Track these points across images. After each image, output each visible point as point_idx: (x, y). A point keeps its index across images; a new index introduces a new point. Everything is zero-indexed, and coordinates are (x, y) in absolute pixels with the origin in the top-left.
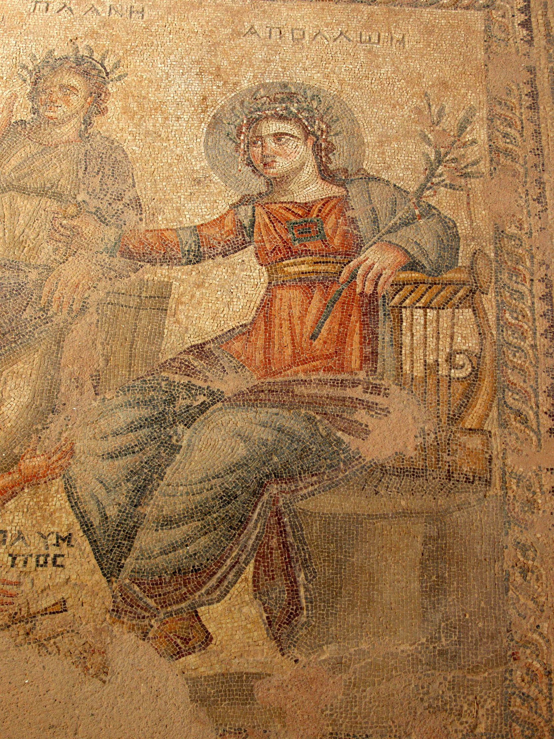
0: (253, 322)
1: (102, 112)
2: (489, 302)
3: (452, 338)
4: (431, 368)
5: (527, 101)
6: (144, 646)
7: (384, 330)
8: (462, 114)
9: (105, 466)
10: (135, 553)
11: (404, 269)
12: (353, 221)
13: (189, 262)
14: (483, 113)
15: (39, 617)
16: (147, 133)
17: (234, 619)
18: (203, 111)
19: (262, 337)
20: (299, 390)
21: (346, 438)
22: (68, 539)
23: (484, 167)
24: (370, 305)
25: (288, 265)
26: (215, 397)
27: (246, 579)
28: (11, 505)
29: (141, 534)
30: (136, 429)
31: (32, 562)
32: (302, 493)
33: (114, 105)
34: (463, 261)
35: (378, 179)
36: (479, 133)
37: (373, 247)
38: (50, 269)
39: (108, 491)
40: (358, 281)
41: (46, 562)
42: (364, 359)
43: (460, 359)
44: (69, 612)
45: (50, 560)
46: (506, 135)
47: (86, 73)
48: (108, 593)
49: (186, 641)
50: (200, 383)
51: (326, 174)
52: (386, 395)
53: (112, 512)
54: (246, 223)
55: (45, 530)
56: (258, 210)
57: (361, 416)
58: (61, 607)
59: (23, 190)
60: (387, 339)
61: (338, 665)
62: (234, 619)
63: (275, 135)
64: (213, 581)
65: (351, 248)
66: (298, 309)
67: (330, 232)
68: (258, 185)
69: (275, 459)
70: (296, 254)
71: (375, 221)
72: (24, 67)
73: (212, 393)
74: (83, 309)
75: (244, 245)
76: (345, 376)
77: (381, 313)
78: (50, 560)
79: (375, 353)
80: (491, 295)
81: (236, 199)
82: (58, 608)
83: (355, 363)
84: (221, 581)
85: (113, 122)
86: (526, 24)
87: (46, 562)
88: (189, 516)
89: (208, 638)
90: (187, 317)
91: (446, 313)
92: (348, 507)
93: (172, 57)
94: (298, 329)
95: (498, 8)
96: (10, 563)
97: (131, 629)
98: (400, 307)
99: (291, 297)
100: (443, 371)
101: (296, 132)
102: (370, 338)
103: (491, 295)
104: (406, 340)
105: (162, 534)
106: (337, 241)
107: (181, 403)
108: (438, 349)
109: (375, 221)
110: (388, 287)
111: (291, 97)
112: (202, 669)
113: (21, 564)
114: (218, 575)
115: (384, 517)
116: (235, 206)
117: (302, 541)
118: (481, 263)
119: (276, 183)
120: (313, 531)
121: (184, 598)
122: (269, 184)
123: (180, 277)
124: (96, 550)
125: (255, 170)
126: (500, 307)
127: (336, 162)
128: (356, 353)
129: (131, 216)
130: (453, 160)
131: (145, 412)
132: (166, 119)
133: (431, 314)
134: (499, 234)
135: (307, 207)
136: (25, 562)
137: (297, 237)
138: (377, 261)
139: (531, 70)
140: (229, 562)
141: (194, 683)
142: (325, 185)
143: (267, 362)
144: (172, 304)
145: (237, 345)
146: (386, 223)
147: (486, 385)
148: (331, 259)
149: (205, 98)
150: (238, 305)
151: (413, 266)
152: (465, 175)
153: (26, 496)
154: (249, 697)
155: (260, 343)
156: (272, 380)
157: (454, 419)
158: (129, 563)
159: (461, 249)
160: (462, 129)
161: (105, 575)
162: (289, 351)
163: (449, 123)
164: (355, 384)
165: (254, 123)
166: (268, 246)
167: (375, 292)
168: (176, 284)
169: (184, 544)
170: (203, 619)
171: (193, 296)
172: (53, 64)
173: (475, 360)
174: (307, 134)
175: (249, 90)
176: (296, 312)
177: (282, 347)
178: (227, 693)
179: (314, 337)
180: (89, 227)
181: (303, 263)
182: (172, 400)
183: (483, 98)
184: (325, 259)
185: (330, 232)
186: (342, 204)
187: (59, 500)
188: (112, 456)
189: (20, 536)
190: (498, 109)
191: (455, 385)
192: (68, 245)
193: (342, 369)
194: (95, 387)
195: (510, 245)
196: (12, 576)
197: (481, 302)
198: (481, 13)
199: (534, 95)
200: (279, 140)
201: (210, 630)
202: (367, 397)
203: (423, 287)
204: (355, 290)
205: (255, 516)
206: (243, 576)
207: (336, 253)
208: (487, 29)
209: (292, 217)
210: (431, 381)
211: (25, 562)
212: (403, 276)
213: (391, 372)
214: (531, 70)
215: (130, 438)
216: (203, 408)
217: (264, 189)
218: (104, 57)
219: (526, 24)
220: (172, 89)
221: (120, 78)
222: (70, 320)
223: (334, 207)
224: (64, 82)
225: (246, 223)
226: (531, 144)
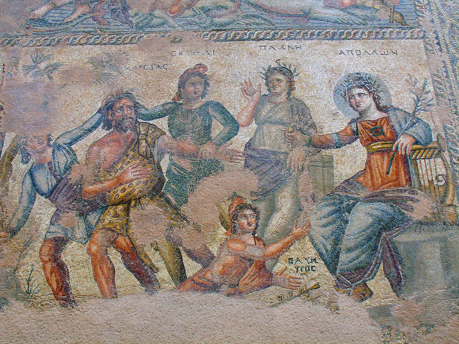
0: (365, 170)
1: (294, 89)
2: (446, 155)
3: (436, 170)
4: (431, 182)
5: (445, 74)
6: (351, 299)
7: (412, 169)
8: (423, 81)
9: (322, 230)
10: (340, 263)
11: (414, 144)
12: (393, 126)
13: (337, 147)
14: (430, 80)
15: (310, 291)
16: (312, 97)
17: (379, 284)
18: (331, 86)
19: (369, 175)
20: (387, 195)
21: (405, 212)
22: (315, 260)
23: (434, 102)
24: (405, 159)
25: (373, 146)
26: (357, 200)
27: (381, 270)
28: (292, 248)
29: (341, 255)
30: (331, 215)
31: (304, 270)
32: (394, 234)
33: (297, 86)
34: (434, 139)
35: (398, 109)
36: (430, 88)
37: (402, 136)
38: (287, 154)
39: (326, 239)
40: (399, 150)
41: (309, 269)
42: (407, 181)
43: (440, 178)
44: (321, 288)
45: (310, 268)
46: (440, 89)
47: (284, 74)
48: (334, 279)
49: (364, 295)
50: (350, 195)
51: (379, 108)
52: (417, 194)
53: (329, 247)
54: (355, 129)
55: (307, 256)
56: (358, 125)
57: (409, 202)
58: (317, 286)
59: (270, 122)
60: (414, 172)
61: (418, 300)
62: (379, 284)
63: (358, 94)
64: (369, 272)
65: (394, 137)
66: (381, 163)
67: (385, 131)
68: (356, 115)
69: (382, 223)
70: (375, 141)
71: (400, 126)
72: (261, 73)
73: (355, 199)
74: (303, 169)
75: (356, 139)
76: (401, 188)
77: (409, 162)
78: (310, 268)
79: (410, 178)
80: (446, 152)
81: (349, 121)
82: (317, 286)
83: (404, 183)
84: (372, 271)
85: (298, 93)
86: (438, 44)
87: (309, 269)
88: (356, 247)
89: (372, 293)
90: (341, 169)
91: (432, 160)
92: (411, 239)
93: (315, 65)
94: (381, 170)
95: (427, 38)
96: (296, 271)
97: (344, 293)
98: (415, 159)
99: (376, 157)
100: (435, 183)
101: (366, 92)
102: (408, 173)
103: (446, 152)
104: (420, 172)
105: (348, 255)
106: (388, 135)
107: (345, 204)
108: (432, 175)
109: (400, 126)
110: (410, 152)
111: (361, 78)
112: (372, 305)
113: (300, 271)
114: (371, 269)
115: (425, 241)
116: (350, 124)
117: (397, 253)
118: (440, 141)
119: (361, 114)
120: (401, 249)
121: (361, 279)
122: (360, 114)
123: (334, 152)
124: (326, 263)
125: (354, 109)
126: (451, 156)
127: (383, 103)
128: (404, 178)
129: (312, 131)
130: (423, 100)
131: (333, 208)
132: (318, 90)
133: (427, 161)
134: (445, 127)
135: (375, 122)
136: (302, 270)
137: (374, 134)
138: (404, 141)
139: (444, 62)
140: (374, 263)
141: (369, 310)
142: (380, 113)
143: (373, 184)
144: (335, 165)
145: (361, 179)
146: (404, 126)
147: (451, 187)
148: (388, 142)
149: (330, 81)
150: (359, 163)
151: (417, 143)
152: (429, 105)
153: (297, 244)
154: (389, 315)
155: (369, 177)
156: (376, 191)
157: (442, 202)
158: (339, 267)
159: (433, 135)
160: (424, 88)
161: (331, 273)
162: (380, 180)
163: (419, 85)
164: (405, 191)
165: (349, 89)
166: (364, 139)
167: (406, 154)
168: (334, 156)
169: (357, 257)
170: (368, 286)
171: (341, 160)
172: (271, 71)
173: (445, 177)
174: (370, 93)
175: (345, 77)
176: (379, 163)
177: (377, 179)
178: (381, 313)
179: (388, 173)
180: (299, 136)
181: (378, 144)
182: (342, 203)
183: (429, 74)
184: (385, 142)
185: (385, 131)
186: (387, 120)
187: (309, 245)
188: (325, 226)
189: (298, 260)
190: (436, 78)
191: (441, 189)
192: (292, 144)
193: (400, 185)
194: (313, 199)
195: (449, 132)
196: (298, 276)
197: (443, 155)
198: (421, 40)
199: (446, 72)
200: (360, 96)
201: (372, 290)
202: (409, 195)
203: (422, 151)
204: (398, 154)
205: (379, 246)
206: (380, 269)
207: (389, 140)
208: (425, 46)
209: (370, 126)
210: (432, 188)
211: (302, 270)
212: (415, 147)
213: (417, 186)
214: (444, 62)
215: (330, 219)
216: (354, 205)
217: (358, 116)
218: (290, 68)
219: (438, 44)
220: (317, 78)
221: (296, 75)
222: (299, 173)
223: (385, 121)
224: (278, 77)
225: (355, 130)
226: (449, 91)
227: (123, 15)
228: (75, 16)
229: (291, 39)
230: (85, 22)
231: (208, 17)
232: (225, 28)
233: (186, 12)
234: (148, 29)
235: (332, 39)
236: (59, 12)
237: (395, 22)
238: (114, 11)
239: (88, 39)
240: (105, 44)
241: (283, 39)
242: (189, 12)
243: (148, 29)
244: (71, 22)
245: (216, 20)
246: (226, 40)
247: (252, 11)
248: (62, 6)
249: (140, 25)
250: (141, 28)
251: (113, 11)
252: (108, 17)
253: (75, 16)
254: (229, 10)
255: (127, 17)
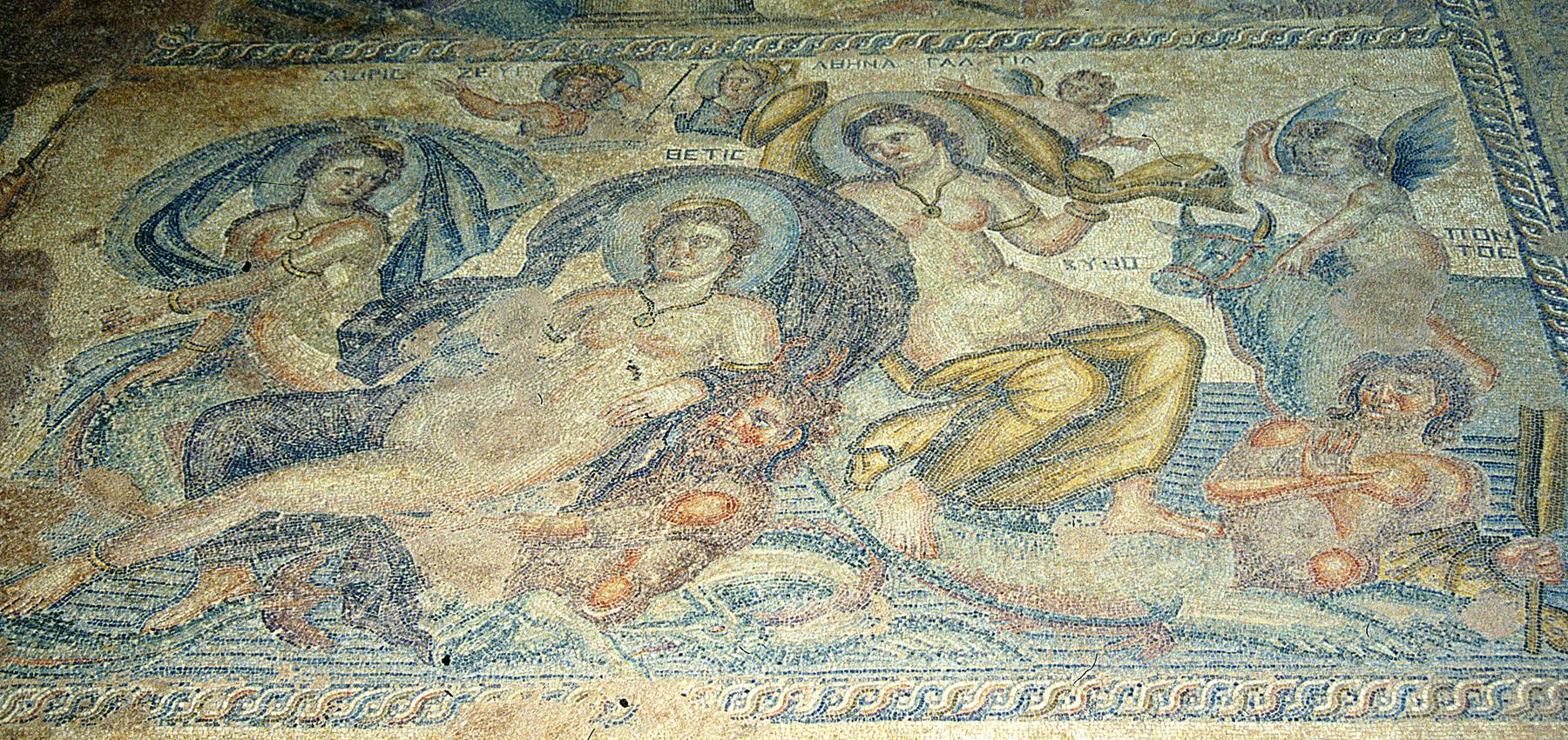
227: (394, 608)
228: (189, 608)
229: (1099, 716)
230: (229, 632)
231: (747, 622)
232: (820, 667)
233: (660, 600)
234: (499, 668)
235: (1276, 715)
236: (126, 588)
237: (1544, 645)
238: (353, 593)
239: (238, 699)
240: (310, 723)
241: (1063, 716)
242: (665, 607)
243: (492, 669)
244: (175, 630)
245: (787, 635)
246: (820, 713)
247: (935, 602)
248: (139, 566)
249: (465, 650)
250: (469, 661)
251: (353, 593)
252: (331, 615)
253: (189, 608)
254: (835, 597)
255: (409, 620)
